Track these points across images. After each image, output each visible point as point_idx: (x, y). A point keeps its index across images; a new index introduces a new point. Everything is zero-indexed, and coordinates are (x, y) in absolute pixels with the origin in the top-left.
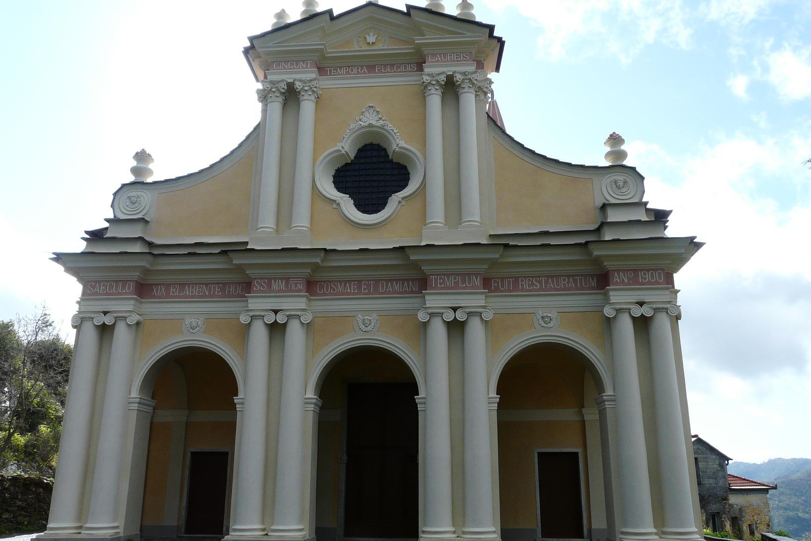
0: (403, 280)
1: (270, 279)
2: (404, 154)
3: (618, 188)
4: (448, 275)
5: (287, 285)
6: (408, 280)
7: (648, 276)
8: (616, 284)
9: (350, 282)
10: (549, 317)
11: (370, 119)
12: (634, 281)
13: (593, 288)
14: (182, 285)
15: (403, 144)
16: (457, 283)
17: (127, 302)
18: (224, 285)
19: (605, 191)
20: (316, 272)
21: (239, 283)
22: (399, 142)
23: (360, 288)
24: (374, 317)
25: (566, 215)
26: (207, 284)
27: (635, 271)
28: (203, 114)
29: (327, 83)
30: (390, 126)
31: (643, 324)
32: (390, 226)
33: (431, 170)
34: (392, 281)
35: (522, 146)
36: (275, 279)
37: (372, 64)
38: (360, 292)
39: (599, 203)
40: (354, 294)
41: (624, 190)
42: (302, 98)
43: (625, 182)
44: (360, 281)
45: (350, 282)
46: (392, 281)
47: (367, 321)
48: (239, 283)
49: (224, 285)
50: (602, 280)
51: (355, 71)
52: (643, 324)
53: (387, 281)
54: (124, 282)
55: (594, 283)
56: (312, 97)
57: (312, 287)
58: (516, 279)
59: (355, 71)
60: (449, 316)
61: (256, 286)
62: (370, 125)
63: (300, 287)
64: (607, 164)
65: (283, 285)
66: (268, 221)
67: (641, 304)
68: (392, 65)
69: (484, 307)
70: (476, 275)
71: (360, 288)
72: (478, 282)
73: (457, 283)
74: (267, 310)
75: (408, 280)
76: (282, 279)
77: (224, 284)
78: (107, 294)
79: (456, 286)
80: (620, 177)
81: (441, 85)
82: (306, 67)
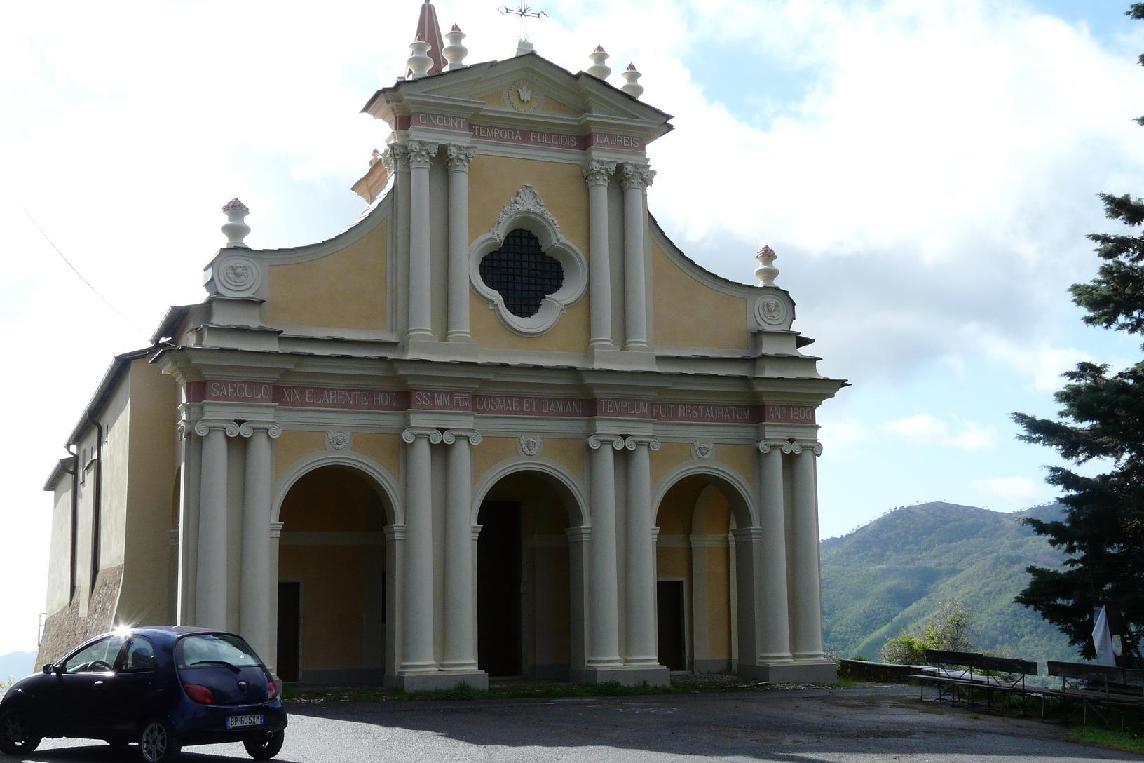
0: (567, 400)
1: (433, 392)
2: (565, 253)
3: (770, 311)
4: (618, 400)
5: (452, 401)
6: (571, 400)
7: (799, 413)
8: (771, 419)
9: (511, 398)
10: (707, 448)
11: (527, 203)
12: (786, 418)
13: (745, 421)
14: (320, 391)
15: (563, 240)
16: (626, 409)
17: (267, 410)
18: (370, 393)
19: (756, 315)
20: (482, 388)
21: (388, 392)
22: (560, 236)
23: (521, 405)
24: (538, 440)
25: (711, 338)
26: (349, 391)
27: (788, 407)
28: (313, 174)
29: (485, 149)
30: (550, 216)
31: (791, 461)
32: (541, 338)
33: (590, 277)
34: (554, 400)
35: (681, 254)
36: (439, 393)
37: (527, 132)
38: (521, 412)
39: (752, 326)
40: (516, 413)
41: (774, 314)
42: (453, 169)
43: (777, 306)
44: (521, 399)
45: (511, 398)
46: (554, 400)
47: (533, 445)
48: (388, 392)
49: (370, 393)
50: (756, 413)
51: (507, 136)
52: (791, 461)
53: (550, 400)
54: (259, 385)
55: (746, 415)
56: (466, 169)
57: (279, 394)
58: (676, 405)
59: (507, 136)
60: (436, 439)
61: (417, 399)
62: (528, 211)
63: (467, 403)
64: (761, 284)
65: (447, 401)
66: (424, 324)
67: (791, 441)
68: (549, 135)
69: (653, 437)
70: (645, 402)
71: (521, 405)
72: (646, 409)
73: (626, 409)
74: (432, 429)
75: (571, 400)
76: (446, 393)
77: (371, 392)
78: (237, 399)
79: (625, 413)
80: (773, 300)
81: (431, 158)
82: (459, 128)
